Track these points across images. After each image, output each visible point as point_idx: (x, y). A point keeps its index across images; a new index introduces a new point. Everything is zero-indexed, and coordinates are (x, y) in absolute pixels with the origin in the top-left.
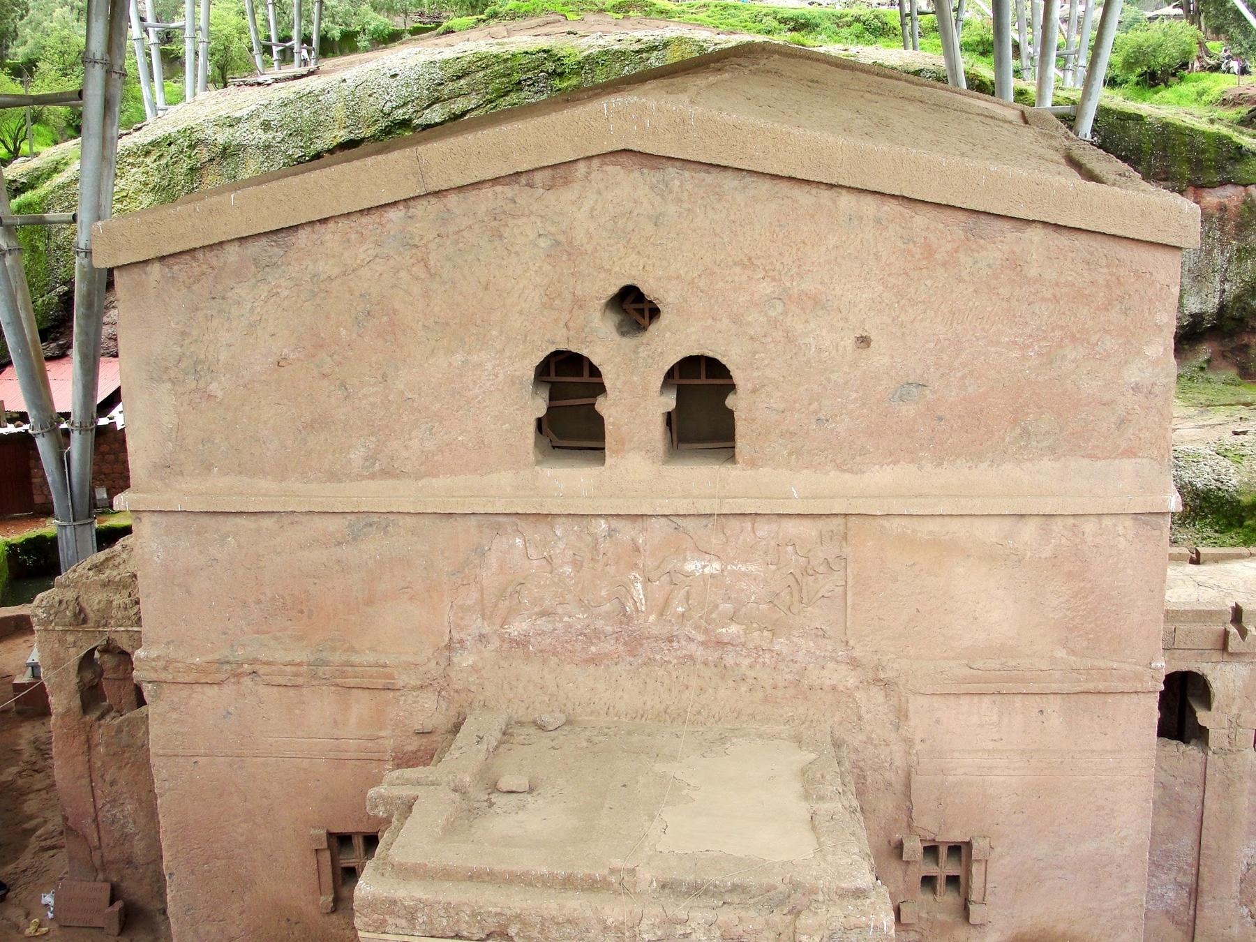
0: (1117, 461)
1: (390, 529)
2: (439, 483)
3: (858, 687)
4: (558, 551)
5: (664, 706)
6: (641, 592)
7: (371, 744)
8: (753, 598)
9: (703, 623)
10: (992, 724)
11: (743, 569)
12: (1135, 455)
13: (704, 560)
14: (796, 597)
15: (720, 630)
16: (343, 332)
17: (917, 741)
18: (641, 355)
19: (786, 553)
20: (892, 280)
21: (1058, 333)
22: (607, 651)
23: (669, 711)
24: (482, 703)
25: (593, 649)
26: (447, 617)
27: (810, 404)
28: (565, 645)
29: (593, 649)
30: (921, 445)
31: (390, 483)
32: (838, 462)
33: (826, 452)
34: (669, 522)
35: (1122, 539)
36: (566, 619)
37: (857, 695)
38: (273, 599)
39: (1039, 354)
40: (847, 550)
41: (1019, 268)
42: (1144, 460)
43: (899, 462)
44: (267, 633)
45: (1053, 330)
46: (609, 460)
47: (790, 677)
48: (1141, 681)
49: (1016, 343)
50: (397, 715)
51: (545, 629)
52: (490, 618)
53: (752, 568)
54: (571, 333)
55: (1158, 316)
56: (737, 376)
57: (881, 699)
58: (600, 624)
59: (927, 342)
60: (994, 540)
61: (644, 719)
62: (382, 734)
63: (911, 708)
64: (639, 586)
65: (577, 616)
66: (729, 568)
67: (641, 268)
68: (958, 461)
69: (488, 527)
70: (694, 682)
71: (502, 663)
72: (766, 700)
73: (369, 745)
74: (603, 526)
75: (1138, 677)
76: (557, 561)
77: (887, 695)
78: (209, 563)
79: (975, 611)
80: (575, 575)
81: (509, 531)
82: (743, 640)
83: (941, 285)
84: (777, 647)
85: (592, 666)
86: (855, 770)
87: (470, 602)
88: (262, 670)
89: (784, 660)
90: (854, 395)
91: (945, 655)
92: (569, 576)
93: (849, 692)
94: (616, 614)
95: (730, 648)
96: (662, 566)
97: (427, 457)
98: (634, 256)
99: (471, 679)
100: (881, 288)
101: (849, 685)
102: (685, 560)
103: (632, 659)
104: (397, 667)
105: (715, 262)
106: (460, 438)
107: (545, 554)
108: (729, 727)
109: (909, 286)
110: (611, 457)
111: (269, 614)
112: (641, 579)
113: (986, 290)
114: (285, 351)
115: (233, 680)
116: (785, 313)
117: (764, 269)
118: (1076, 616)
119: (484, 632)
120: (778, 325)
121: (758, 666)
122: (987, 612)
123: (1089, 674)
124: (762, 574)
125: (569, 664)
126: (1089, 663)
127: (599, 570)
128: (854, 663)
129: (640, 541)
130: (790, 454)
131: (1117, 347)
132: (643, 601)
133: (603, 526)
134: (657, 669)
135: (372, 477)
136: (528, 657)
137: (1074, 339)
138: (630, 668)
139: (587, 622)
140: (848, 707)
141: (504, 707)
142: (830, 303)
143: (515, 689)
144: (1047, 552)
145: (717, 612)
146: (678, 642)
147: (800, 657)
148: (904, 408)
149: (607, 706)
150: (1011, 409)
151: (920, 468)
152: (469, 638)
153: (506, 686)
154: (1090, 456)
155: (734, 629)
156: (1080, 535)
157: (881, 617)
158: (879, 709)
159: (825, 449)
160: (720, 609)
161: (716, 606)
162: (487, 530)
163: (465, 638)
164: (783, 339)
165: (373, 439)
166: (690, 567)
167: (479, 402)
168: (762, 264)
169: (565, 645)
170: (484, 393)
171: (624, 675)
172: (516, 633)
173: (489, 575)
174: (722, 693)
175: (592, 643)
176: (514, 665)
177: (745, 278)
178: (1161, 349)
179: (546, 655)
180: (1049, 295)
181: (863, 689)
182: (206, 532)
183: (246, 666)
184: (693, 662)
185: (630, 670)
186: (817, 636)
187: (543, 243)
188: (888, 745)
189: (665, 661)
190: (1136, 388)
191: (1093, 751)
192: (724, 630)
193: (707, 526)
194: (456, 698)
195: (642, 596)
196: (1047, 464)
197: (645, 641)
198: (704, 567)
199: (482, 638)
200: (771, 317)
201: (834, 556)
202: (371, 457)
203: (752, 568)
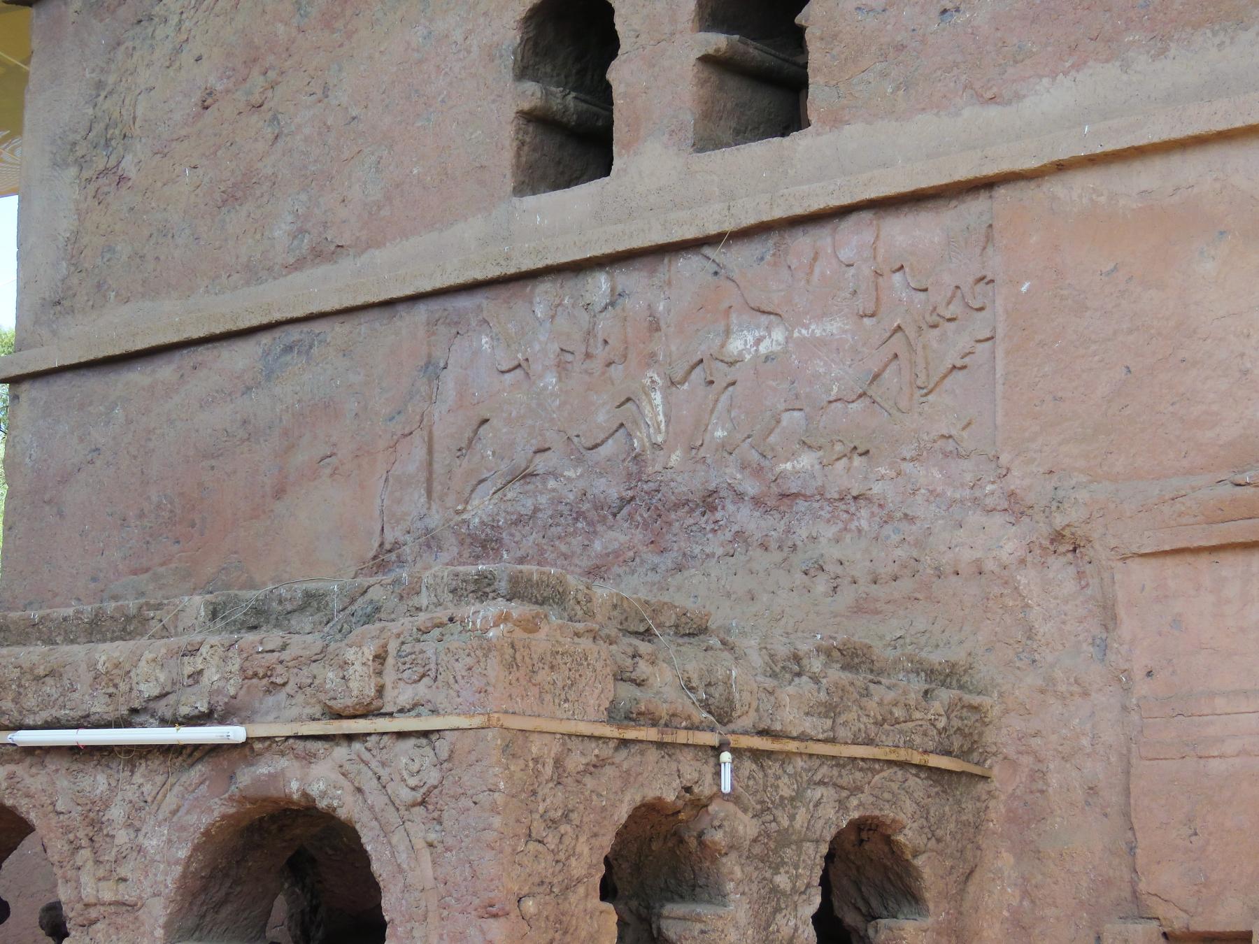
1: (315, 351)
3: (1022, 562)
6: (660, 408)
8: (835, 389)
9: (754, 456)
11: (818, 333)
13: (758, 327)
15: (782, 466)
17: (1139, 674)
26: (379, 501)
28: (557, 543)
29: (598, 546)
32: (977, 85)
33: (955, 71)
34: (704, 261)
36: (552, 484)
37: (1026, 579)
40: (995, 263)
43: (1085, 63)
57: (1070, 586)
63: (1121, 595)
64: (658, 398)
65: (566, 473)
66: (796, 334)
69: (443, 324)
74: (604, 287)
77: (1080, 575)
78: (89, 458)
79: (1242, 355)
86: (1027, 760)
93: (1006, 573)
94: (621, 458)
101: (1004, 555)
102: (728, 332)
103: (656, 559)
107: (520, 356)
112: (661, 384)
124: (849, 337)
128: (1016, 507)
129: (661, 308)
132: (663, 426)
135: (299, 264)
139: (581, 484)
140: (1004, 607)
145: (777, 430)
147: (920, 508)
151: (1126, 67)
152: (408, 538)
155: (806, 461)
157: (1060, 394)
159: (956, 64)
160: (784, 423)
163: (401, 539)
165: (304, 197)
166: (736, 345)
169: (557, 543)
172: (477, 520)
186: (946, 455)
188: (1085, 694)
192: (789, 466)
193: (762, 259)
195: (661, 418)
197: (673, 516)
198: (758, 341)
201: (971, 279)
203: (833, 327)
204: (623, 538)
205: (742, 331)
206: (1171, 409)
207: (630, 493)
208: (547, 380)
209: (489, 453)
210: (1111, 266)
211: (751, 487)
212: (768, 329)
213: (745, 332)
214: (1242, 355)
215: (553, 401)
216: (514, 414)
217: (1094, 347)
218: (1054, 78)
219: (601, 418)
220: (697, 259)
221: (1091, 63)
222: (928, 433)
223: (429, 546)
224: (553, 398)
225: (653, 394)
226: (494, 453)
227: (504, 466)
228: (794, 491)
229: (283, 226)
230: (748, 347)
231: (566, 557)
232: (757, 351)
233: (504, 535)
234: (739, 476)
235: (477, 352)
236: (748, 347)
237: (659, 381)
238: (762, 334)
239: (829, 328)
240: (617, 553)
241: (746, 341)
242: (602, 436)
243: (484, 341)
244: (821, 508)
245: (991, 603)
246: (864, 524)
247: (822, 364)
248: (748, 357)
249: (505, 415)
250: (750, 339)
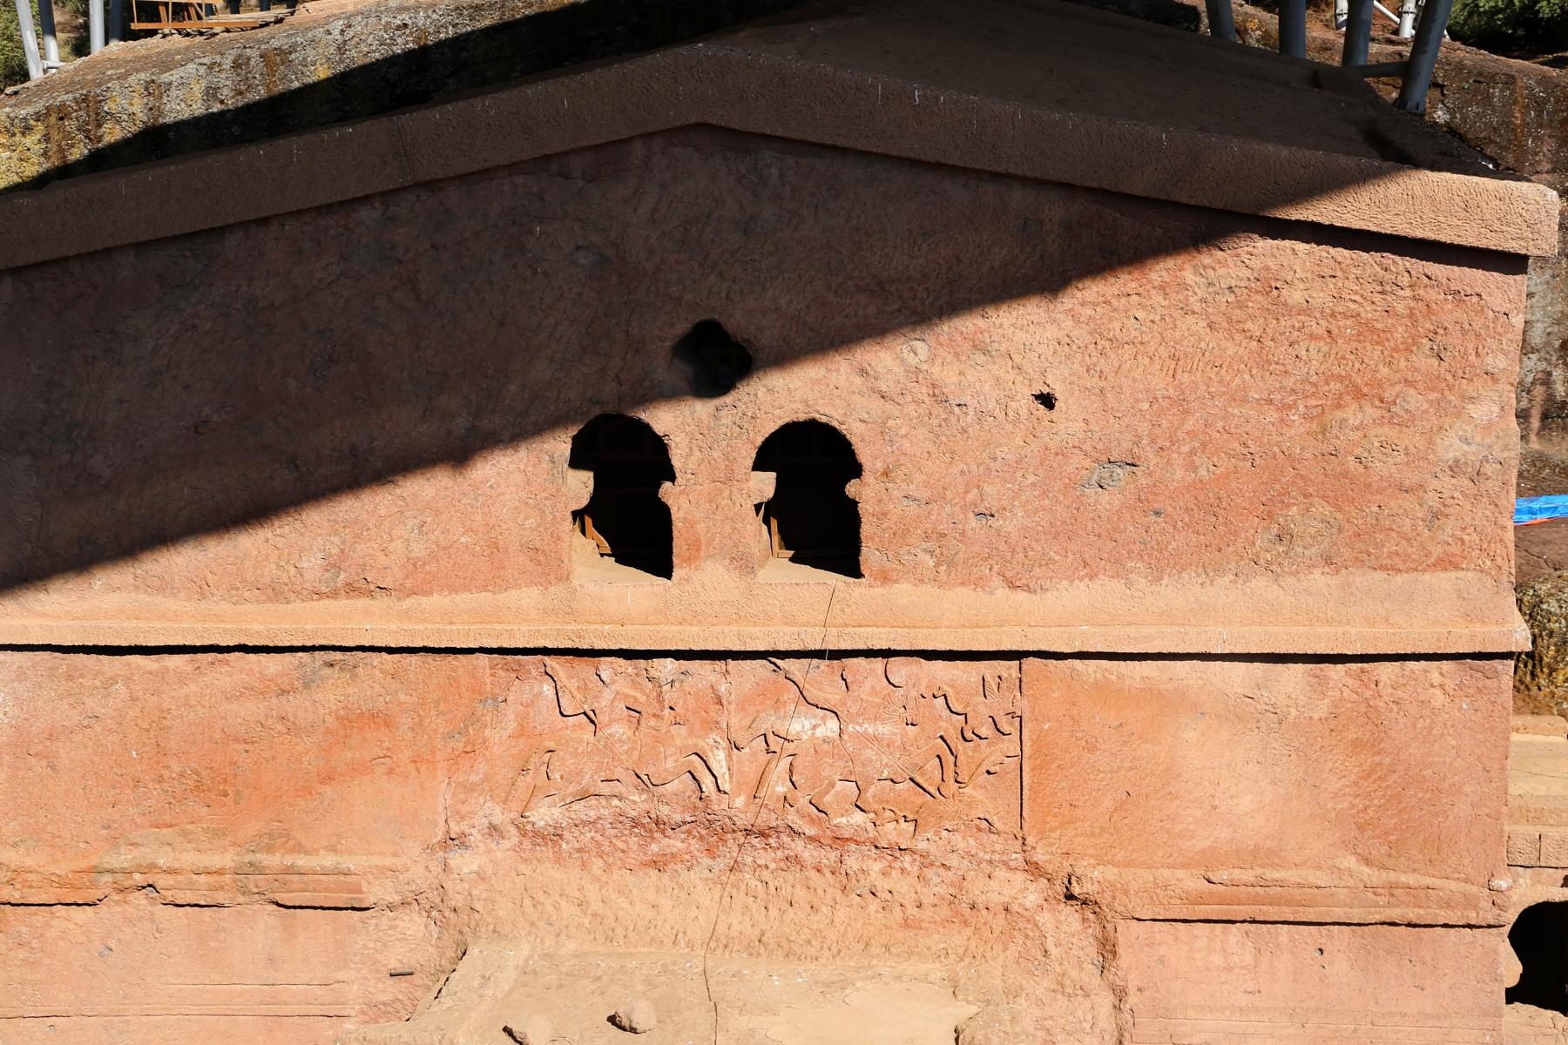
0: (1427, 576)
1: (360, 670)
2: (436, 602)
4: (604, 704)
5: (757, 932)
6: (724, 763)
7: (319, 991)
10: (1245, 967)
11: (871, 731)
12: (1457, 567)
13: (814, 717)
14: (949, 775)
15: (838, 820)
16: (292, 384)
17: (1132, 989)
18: (724, 421)
19: (933, 707)
20: (1088, 311)
21: (1335, 386)
22: (674, 850)
23: (765, 939)
24: (491, 927)
25: (655, 848)
26: (441, 800)
27: (967, 492)
29: (655, 848)
30: (1130, 552)
31: (362, 602)
32: (1008, 575)
35: (1438, 692)
36: (615, 802)
38: (182, 775)
39: (1305, 417)
40: (1022, 705)
41: (1275, 292)
42: (1470, 575)
43: (1096, 575)
44: (171, 826)
45: (1327, 383)
46: (677, 573)
47: (942, 890)
48: (1476, 908)
49: (1270, 402)
50: (365, 947)
52: (505, 802)
53: (885, 729)
54: (623, 388)
55: (1489, 360)
56: (864, 454)
58: (664, 811)
59: (1137, 401)
60: (1240, 691)
61: (727, 952)
62: (340, 975)
63: (1121, 940)
64: (721, 755)
65: (631, 798)
66: (850, 728)
67: (723, 295)
68: (1185, 575)
69: (501, 668)
70: (801, 894)
71: (522, 868)
72: (906, 924)
73: (320, 992)
75: (1470, 902)
76: (601, 719)
78: (86, 723)
79: (1213, 796)
80: (629, 739)
81: (534, 673)
82: (871, 835)
83: (1157, 318)
84: (921, 845)
85: (653, 873)
86: (1039, 1033)
87: (475, 778)
88: (161, 881)
89: (932, 864)
90: (1031, 479)
91: (1170, 861)
92: (620, 741)
95: (853, 847)
96: (754, 725)
97: (414, 566)
98: (713, 278)
99: (475, 892)
100: (1070, 323)
101: (1028, 905)
103: (711, 862)
104: (365, 873)
105: (830, 288)
106: (463, 540)
108: (852, 964)
109: (1111, 320)
110: (682, 567)
111: (174, 798)
113: (1225, 324)
114: (206, 411)
115: (116, 898)
116: (931, 360)
117: (900, 297)
118: (1369, 806)
119: (496, 821)
120: (921, 376)
121: (894, 872)
122: (1231, 797)
123: (1392, 895)
125: (620, 869)
126: (1392, 876)
127: (663, 731)
128: (1034, 869)
129: (723, 689)
130: (937, 565)
131: (1426, 406)
132: (727, 777)
133: (670, 667)
134: (747, 876)
135: (334, 594)
136: (559, 860)
137: (1359, 395)
138: (710, 875)
139: (646, 807)
140: (1027, 936)
141: (524, 933)
142: (996, 345)
143: (539, 907)
144: (1323, 708)
145: (832, 793)
146: (778, 837)
147: (953, 861)
148: (1105, 497)
149: (674, 932)
150: (1264, 499)
151: (1129, 585)
152: (472, 831)
153: (528, 903)
154: (1384, 568)
156: (1373, 686)
157: (1075, 803)
158: (1074, 940)
161: (832, 785)
162: (501, 673)
163: (467, 832)
164: (926, 399)
165: (336, 540)
167: (491, 487)
168: (897, 290)
169: (614, 840)
170: (499, 474)
171: (700, 886)
172: (543, 823)
173: (504, 738)
174: (842, 914)
175: (653, 838)
176: (538, 870)
177: (871, 310)
178: (1496, 409)
179: (586, 856)
180: (1321, 331)
181: (1049, 910)
182: (82, 676)
183: (137, 876)
184: (799, 867)
185: (706, 880)
187: (584, 259)
189: (760, 866)
190: (1455, 469)
191: (1404, 1015)
192: (844, 820)
194: (453, 921)
195: (725, 770)
196: (1319, 579)
198: (814, 727)
199: (494, 830)
200: (911, 366)
201: (1002, 713)
202: (334, 566)
203: (885, 729)
204: (679, 845)
206: (1160, 824)
207: (693, 819)
208: (614, 729)
209: (557, 776)
210: (1117, 723)
211: (810, 831)
212: (823, 718)
214: (1213, 796)
216: (581, 749)
217: (1101, 775)
218: (1072, 582)
219: (670, 764)
221: (1100, 576)
223: (491, 835)
226: (562, 778)
227: (572, 789)
228: (847, 836)
229: (312, 559)
231: (623, 851)
233: (565, 833)
235: (540, 694)
237: (721, 742)
239: (880, 729)
240: (673, 855)
242: (670, 778)
244: (870, 850)
245: (1015, 933)
246: (907, 865)
248: (805, 737)
250: (807, 725)
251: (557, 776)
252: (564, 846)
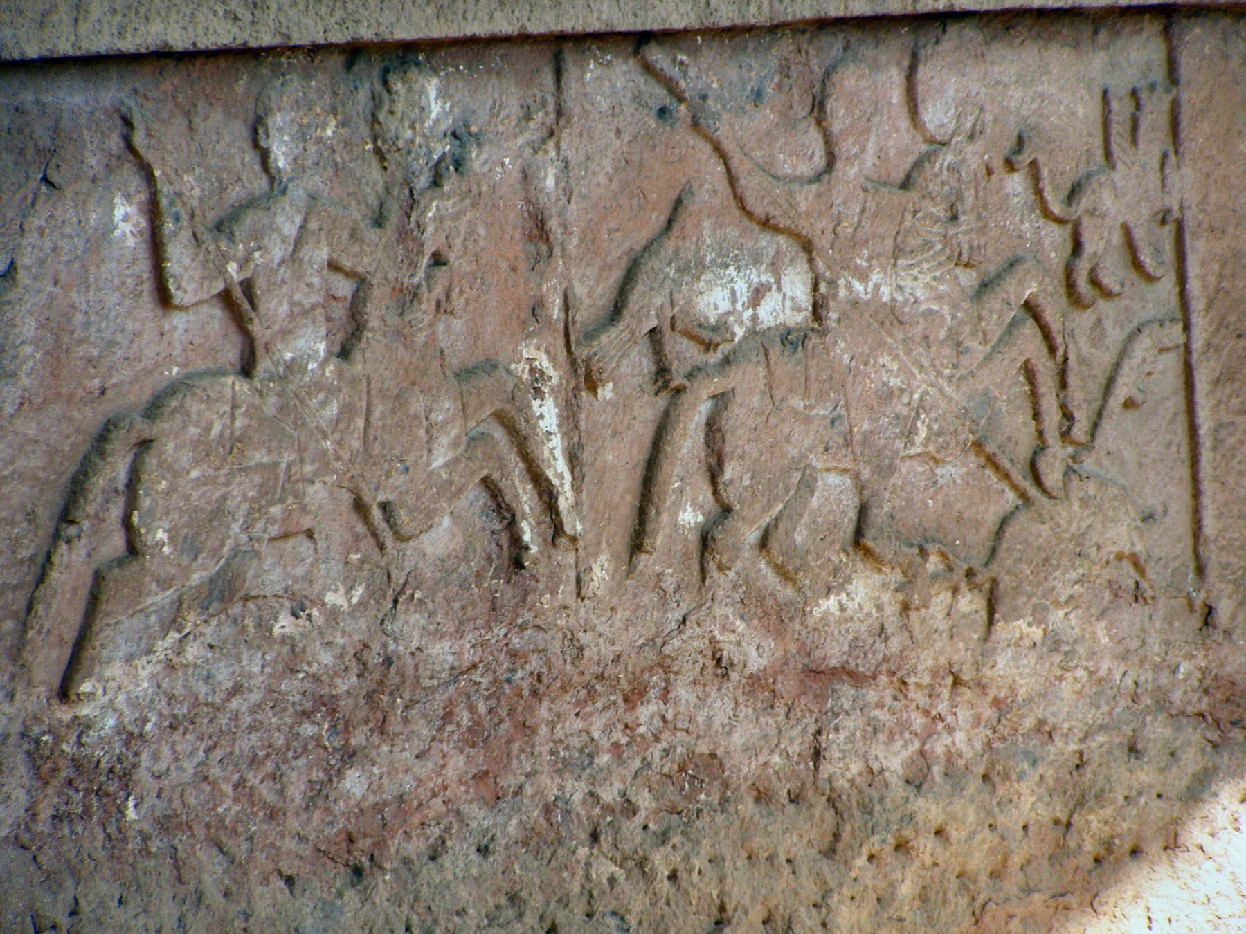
6: (557, 442)
13: (756, 260)
14: (1052, 418)
51: (202, 689)
66: (842, 293)
74: (435, 109)
92: (317, 386)
112: (555, 381)
124: (946, 310)
172: (111, 722)
195: (561, 465)
198: (757, 295)
205: (726, 266)
208: (301, 343)
209: (161, 535)
213: (732, 270)
215: (324, 404)
216: (216, 430)
220: (624, 68)
222: (1099, 548)
224: (321, 396)
225: (536, 404)
230: (739, 307)
232: (755, 318)
234: (740, 626)
236: (739, 307)
237: (551, 372)
238: (764, 278)
241: (733, 292)
243: (119, 212)
247: (895, 367)
249: (193, 431)
250: (741, 286)
251: (161, 535)
252: (131, 814)
